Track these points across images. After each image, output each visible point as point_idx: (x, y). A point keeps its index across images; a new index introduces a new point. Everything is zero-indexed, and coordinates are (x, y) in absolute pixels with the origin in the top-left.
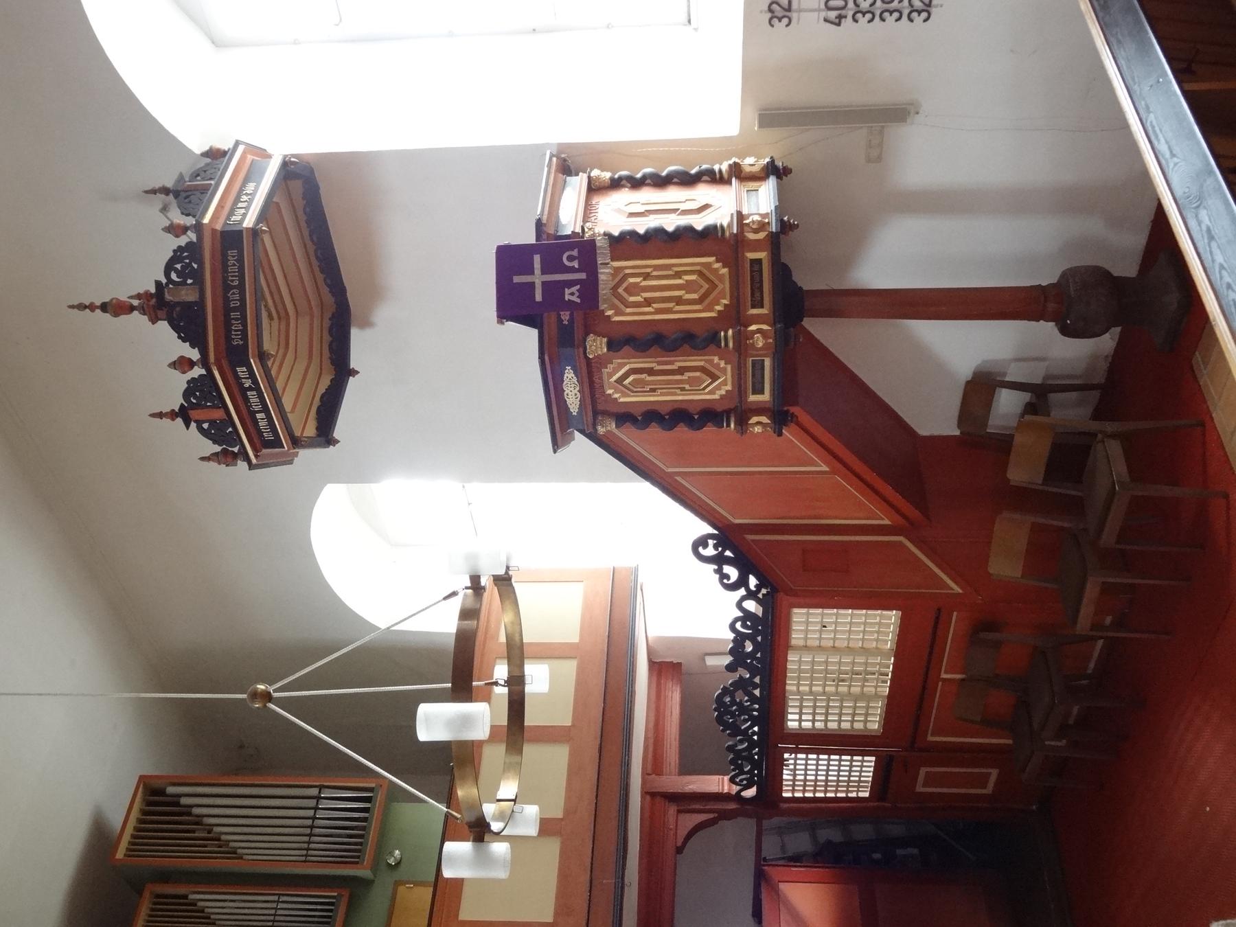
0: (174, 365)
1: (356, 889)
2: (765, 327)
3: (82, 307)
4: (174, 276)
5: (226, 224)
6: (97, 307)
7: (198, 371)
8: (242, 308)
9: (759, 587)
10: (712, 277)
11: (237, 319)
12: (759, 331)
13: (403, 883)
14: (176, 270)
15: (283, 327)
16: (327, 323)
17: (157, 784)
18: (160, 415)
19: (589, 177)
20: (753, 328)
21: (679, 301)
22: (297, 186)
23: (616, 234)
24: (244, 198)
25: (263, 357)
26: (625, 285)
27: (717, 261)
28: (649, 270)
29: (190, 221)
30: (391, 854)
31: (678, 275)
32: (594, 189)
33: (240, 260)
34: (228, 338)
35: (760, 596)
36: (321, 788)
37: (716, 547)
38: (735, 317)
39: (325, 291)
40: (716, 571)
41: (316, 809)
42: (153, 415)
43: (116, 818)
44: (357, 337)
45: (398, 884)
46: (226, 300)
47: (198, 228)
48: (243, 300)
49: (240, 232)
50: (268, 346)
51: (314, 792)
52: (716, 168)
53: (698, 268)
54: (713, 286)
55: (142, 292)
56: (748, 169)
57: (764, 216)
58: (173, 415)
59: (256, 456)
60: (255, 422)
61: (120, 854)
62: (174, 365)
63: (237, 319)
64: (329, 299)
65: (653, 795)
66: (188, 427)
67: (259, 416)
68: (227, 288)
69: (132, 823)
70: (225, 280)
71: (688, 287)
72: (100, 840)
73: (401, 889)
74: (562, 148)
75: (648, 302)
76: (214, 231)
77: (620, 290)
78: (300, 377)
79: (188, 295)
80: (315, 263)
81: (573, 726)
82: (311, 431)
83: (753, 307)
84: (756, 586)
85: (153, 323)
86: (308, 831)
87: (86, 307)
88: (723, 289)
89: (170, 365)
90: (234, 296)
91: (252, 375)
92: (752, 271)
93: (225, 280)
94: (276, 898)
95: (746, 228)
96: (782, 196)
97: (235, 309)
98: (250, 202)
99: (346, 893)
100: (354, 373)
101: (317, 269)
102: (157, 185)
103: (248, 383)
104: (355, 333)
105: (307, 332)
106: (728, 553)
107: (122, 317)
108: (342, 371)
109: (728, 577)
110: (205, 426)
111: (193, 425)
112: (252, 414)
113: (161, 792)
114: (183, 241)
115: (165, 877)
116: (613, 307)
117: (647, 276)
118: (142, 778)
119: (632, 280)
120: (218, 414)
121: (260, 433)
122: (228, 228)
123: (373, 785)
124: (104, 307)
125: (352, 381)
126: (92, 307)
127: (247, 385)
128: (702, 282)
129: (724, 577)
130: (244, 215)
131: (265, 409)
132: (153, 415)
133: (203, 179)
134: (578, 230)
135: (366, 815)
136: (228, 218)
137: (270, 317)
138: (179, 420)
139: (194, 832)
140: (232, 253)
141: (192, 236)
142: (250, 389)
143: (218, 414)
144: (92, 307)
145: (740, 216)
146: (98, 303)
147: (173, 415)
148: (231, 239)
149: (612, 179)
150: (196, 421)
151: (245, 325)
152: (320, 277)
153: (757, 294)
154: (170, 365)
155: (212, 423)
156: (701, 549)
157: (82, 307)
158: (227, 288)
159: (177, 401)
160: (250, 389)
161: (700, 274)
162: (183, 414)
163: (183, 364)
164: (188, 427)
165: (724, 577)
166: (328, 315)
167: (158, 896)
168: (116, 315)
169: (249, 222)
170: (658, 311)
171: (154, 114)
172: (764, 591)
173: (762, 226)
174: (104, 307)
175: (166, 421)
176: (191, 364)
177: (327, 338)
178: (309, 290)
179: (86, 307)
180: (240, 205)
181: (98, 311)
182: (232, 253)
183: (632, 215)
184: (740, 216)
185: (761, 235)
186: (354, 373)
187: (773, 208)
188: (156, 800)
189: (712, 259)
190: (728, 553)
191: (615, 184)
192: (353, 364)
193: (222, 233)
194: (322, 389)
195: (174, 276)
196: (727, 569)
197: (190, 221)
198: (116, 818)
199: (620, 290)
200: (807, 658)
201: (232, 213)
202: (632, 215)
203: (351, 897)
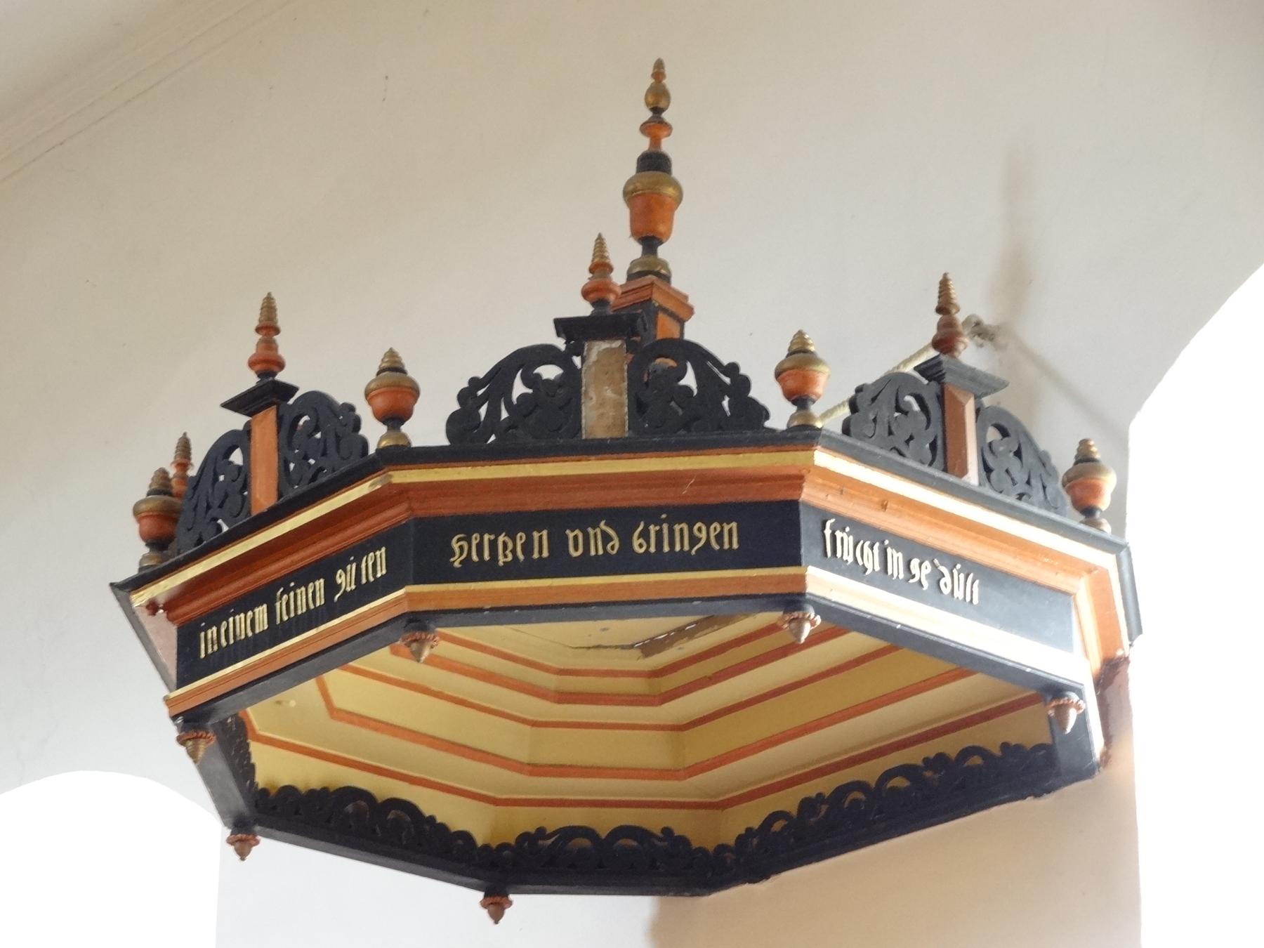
0: (393, 366)
3: (658, 100)
5: (823, 516)
6: (656, 141)
7: (374, 433)
8: (559, 565)
11: (527, 548)
16: (654, 821)
18: (268, 328)
22: (1024, 729)
24: (922, 570)
25: (416, 625)
29: (829, 412)
33: (709, 559)
34: (469, 524)
39: (752, 816)
42: (269, 307)
46: (585, 518)
47: (803, 435)
48: (587, 566)
49: (796, 561)
50: (447, 643)
58: (267, 363)
59: (152, 607)
60: (245, 603)
62: (393, 366)
63: (527, 548)
64: (733, 826)
66: (235, 405)
67: (261, 612)
70: (651, 514)
76: (797, 480)
79: (603, 407)
80: (825, 785)
82: (274, 768)
87: (657, 111)
89: (392, 354)
90: (600, 540)
91: (365, 593)
93: (651, 514)
97: (558, 544)
100: (496, 904)
101: (810, 789)
103: (346, 580)
105: (618, 764)
108: (502, 869)
110: (237, 457)
111: (238, 421)
112: (265, 595)
114: (767, 391)
120: (263, 495)
121: (217, 616)
122: (807, 524)
124: (654, 163)
125: (465, 900)
126: (656, 126)
127: (341, 578)
130: (856, 571)
131: (277, 633)
132: (269, 307)
133: (986, 450)
136: (843, 522)
137: (650, 647)
138: (250, 380)
140: (730, 534)
141: (780, 415)
142: (331, 587)
143: (263, 495)
144: (656, 126)
146: (667, 146)
147: (267, 363)
148: (774, 529)
150: (248, 430)
151: (513, 571)
152: (789, 801)
154: (392, 354)
155: (243, 477)
157: (658, 100)
158: (624, 519)
159: (300, 375)
160: (331, 587)
162: (267, 394)
163: (396, 395)
164: (235, 405)
166: (681, 823)
168: (630, 195)
169: (821, 582)
174: (654, 163)
175: (250, 343)
176: (395, 417)
177: (605, 822)
178: (742, 762)
179: (657, 111)
180: (896, 558)
181: (644, 144)
182: (730, 534)
186: (496, 904)
192: (523, 905)
193: (792, 507)
194: (431, 804)
197: (829, 412)
201: (863, 531)
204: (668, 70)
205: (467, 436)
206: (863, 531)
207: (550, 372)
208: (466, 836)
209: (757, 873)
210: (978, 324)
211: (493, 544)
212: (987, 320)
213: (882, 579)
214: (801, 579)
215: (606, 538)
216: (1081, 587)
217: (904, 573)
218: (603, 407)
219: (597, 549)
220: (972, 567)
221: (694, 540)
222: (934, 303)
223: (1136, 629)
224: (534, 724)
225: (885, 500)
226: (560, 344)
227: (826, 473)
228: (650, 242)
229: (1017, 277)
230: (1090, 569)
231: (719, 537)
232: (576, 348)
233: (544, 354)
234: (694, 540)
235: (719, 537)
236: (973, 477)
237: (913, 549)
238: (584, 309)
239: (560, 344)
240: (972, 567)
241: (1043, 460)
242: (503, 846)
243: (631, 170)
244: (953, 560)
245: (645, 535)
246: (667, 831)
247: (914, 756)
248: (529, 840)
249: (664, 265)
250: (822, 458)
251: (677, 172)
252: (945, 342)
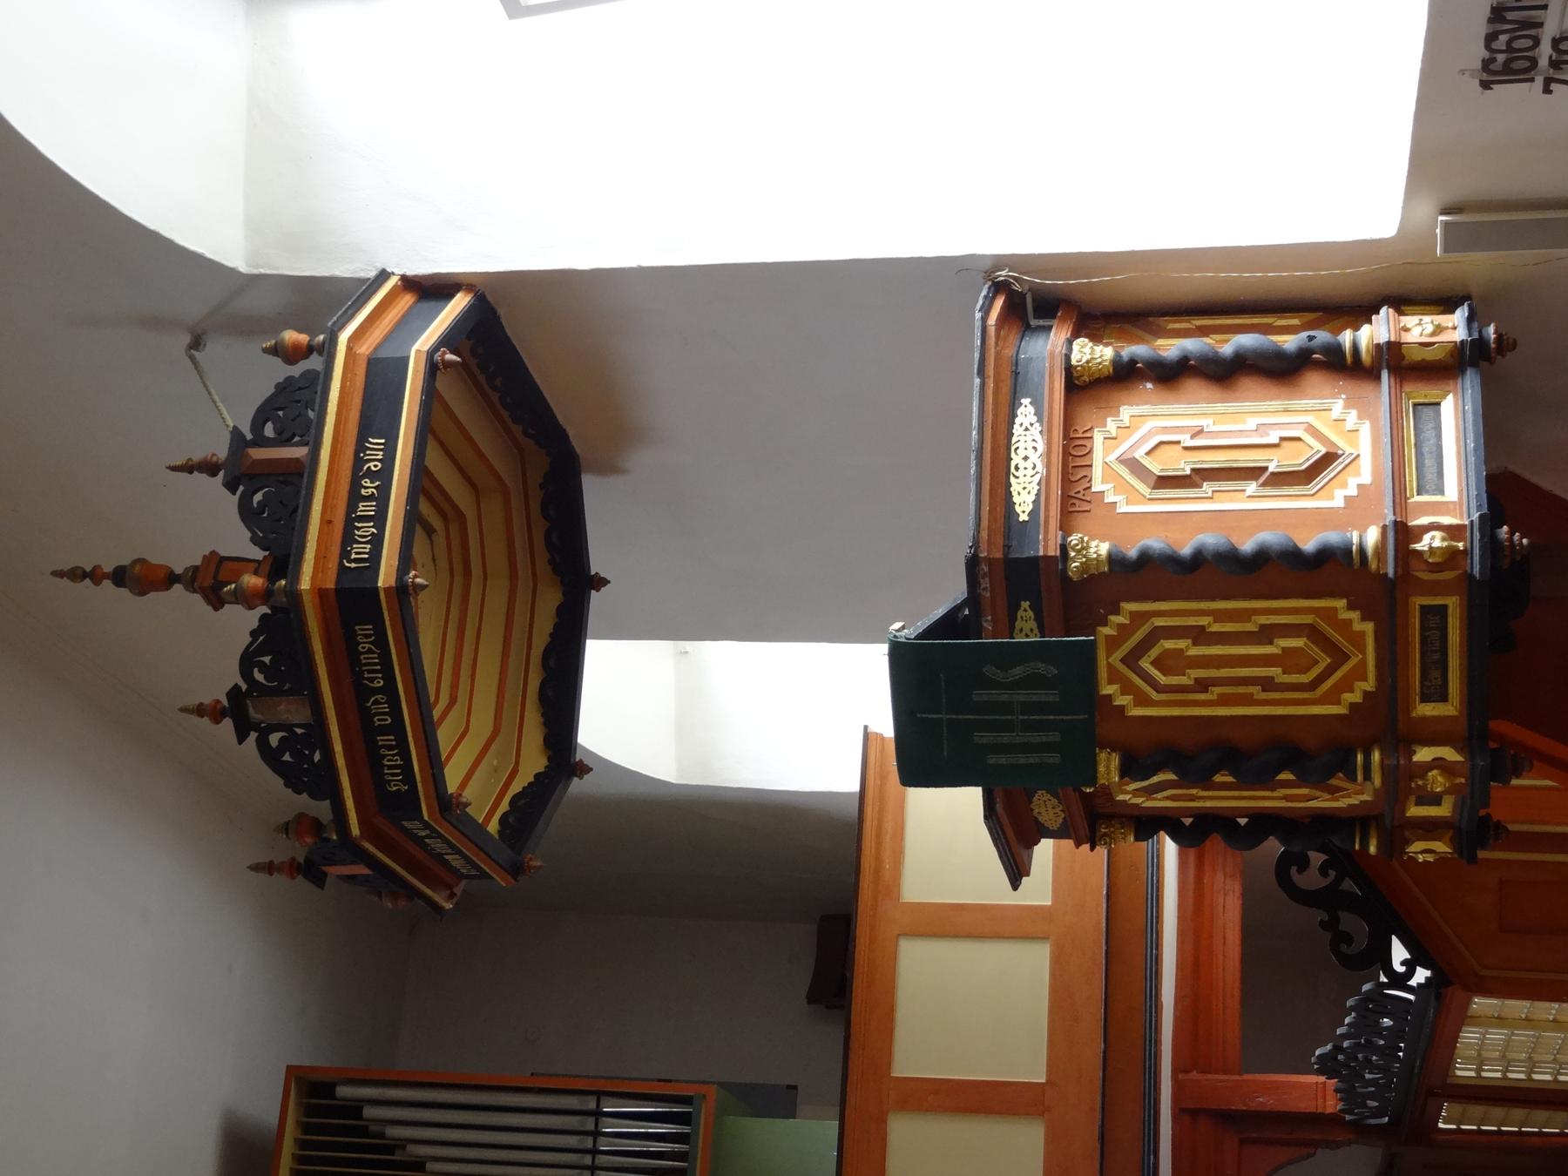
2: (1449, 754)
3: (77, 575)
4: (259, 677)
5: (342, 569)
6: (106, 576)
8: (398, 728)
9: (1411, 966)
10: (1337, 638)
12: (1438, 763)
14: (263, 668)
15: (455, 543)
19: (1069, 369)
20: (1423, 755)
21: (1267, 684)
23: (1133, 553)
24: (369, 487)
26: (1154, 653)
27: (1350, 607)
28: (1203, 621)
31: (1266, 634)
32: (1083, 388)
34: (380, 782)
35: (1413, 982)
36: (600, 1095)
37: (1323, 870)
38: (1384, 721)
40: (1324, 925)
44: (601, 501)
46: (366, 716)
52: (1346, 337)
53: (1307, 619)
54: (1340, 657)
55: (207, 701)
56: (1418, 356)
57: (1452, 532)
63: (390, 748)
65: (1194, 1113)
68: (363, 693)
71: (1287, 660)
74: (1000, 261)
75: (1203, 685)
77: (1145, 664)
78: (502, 618)
81: (1049, 1082)
83: (1425, 699)
84: (1403, 964)
85: (216, 609)
88: (1363, 663)
92: (1423, 629)
95: (1414, 564)
96: (1495, 432)
97: (384, 730)
98: (382, 498)
102: (197, 456)
104: (594, 491)
106: (1348, 885)
107: (152, 595)
109: (1348, 939)
116: (1127, 688)
117: (1200, 635)
118: (290, 1069)
119: (1169, 644)
124: (120, 577)
125: (596, 598)
126: (95, 576)
128: (1316, 651)
129: (1340, 939)
130: (377, 541)
134: (1054, 551)
135: (686, 1129)
136: (345, 554)
144: (95, 576)
145: (1403, 533)
146: (108, 568)
149: (1117, 363)
152: (517, 430)
153: (1435, 674)
156: (1294, 869)
157: (77, 575)
161: (1312, 632)
165: (1340, 939)
168: (142, 593)
170: (1224, 701)
171: (152, 227)
172: (1421, 975)
173: (1451, 557)
174: (120, 577)
176: (317, 826)
177: (540, 526)
181: (107, 583)
183: (1165, 482)
184: (1403, 533)
185: (1448, 575)
187: (1476, 516)
189: (1340, 603)
190: (1348, 885)
191: (1125, 375)
192: (597, 566)
194: (540, 641)
195: (259, 677)
196: (1349, 922)
199: (1145, 664)
200: (1496, 1036)
201: (348, 538)
202: (1165, 482)
204: (58, 568)
205: (321, 783)
206: (348, 538)
207: (274, 739)
208: (559, 610)
209: (563, 436)
210: (191, 347)
211: (390, 767)
212: (187, 339)
213: (380, 519)
214: (386, 589)
215: (376, 702)
216: (364, 349)
217: (371, 502)
218: (293, 712)
219: (385, 708)
220: (361, 447)
221: (370, 651)
222: (185, 475)
223: (384, 275)
224: (485, 579)
225: (326, 522)
226: (253, 735)
227: (313, 578)
228: (170, 579)
229: (156, 323)
230: (349, 349)
231: (367, 636)
232: (256, 727)
233: (263, 744)
234: (370, 651)
235: (367, 636)
236: (299, 452)
237: (355, 497)
238: (228, 724)
239: (253, 735)
240: (361, 447)
241: (285, 387)
242: (562, 582)
243: (124, 592)
244: (358, 462)
245: (372, 680)
246: (541, 486)
247: (481, 378)
248: (556, 569)
249: (187, 569)
250: (305, 584)
251: (126, 562)
252: (210, 468)
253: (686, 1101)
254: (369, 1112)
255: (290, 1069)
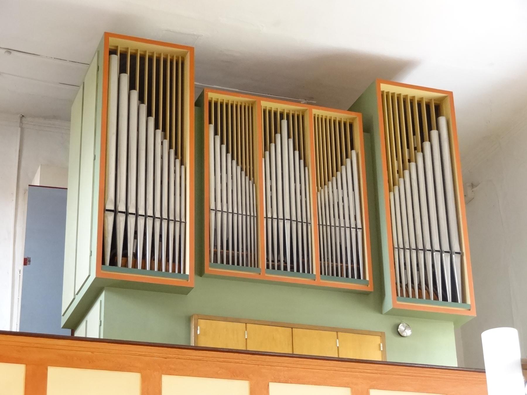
1: (375, 297)
13: (383, 340)
17: (446, 108)
30: (408, 327)
41: (441, 251)
43: (412, 78)
45: (382, 335)
51: (456, 248)
61: (385, 87)
69: (410, 93)
72: (392, 69)
73: (377, 340)
86: (420, 247)
94: (359, 226)
99: (370, 288)
113: (438, 113)
115: (368, 129)
118: (451, 93)
123: (469, 301)
139: (408, 147)
167: (351, 126)
188: (429, 113)
198: (412, 78)
203: (365, 294)
253: (464, 300)
254: (434, 133)
255: (451, 93)
